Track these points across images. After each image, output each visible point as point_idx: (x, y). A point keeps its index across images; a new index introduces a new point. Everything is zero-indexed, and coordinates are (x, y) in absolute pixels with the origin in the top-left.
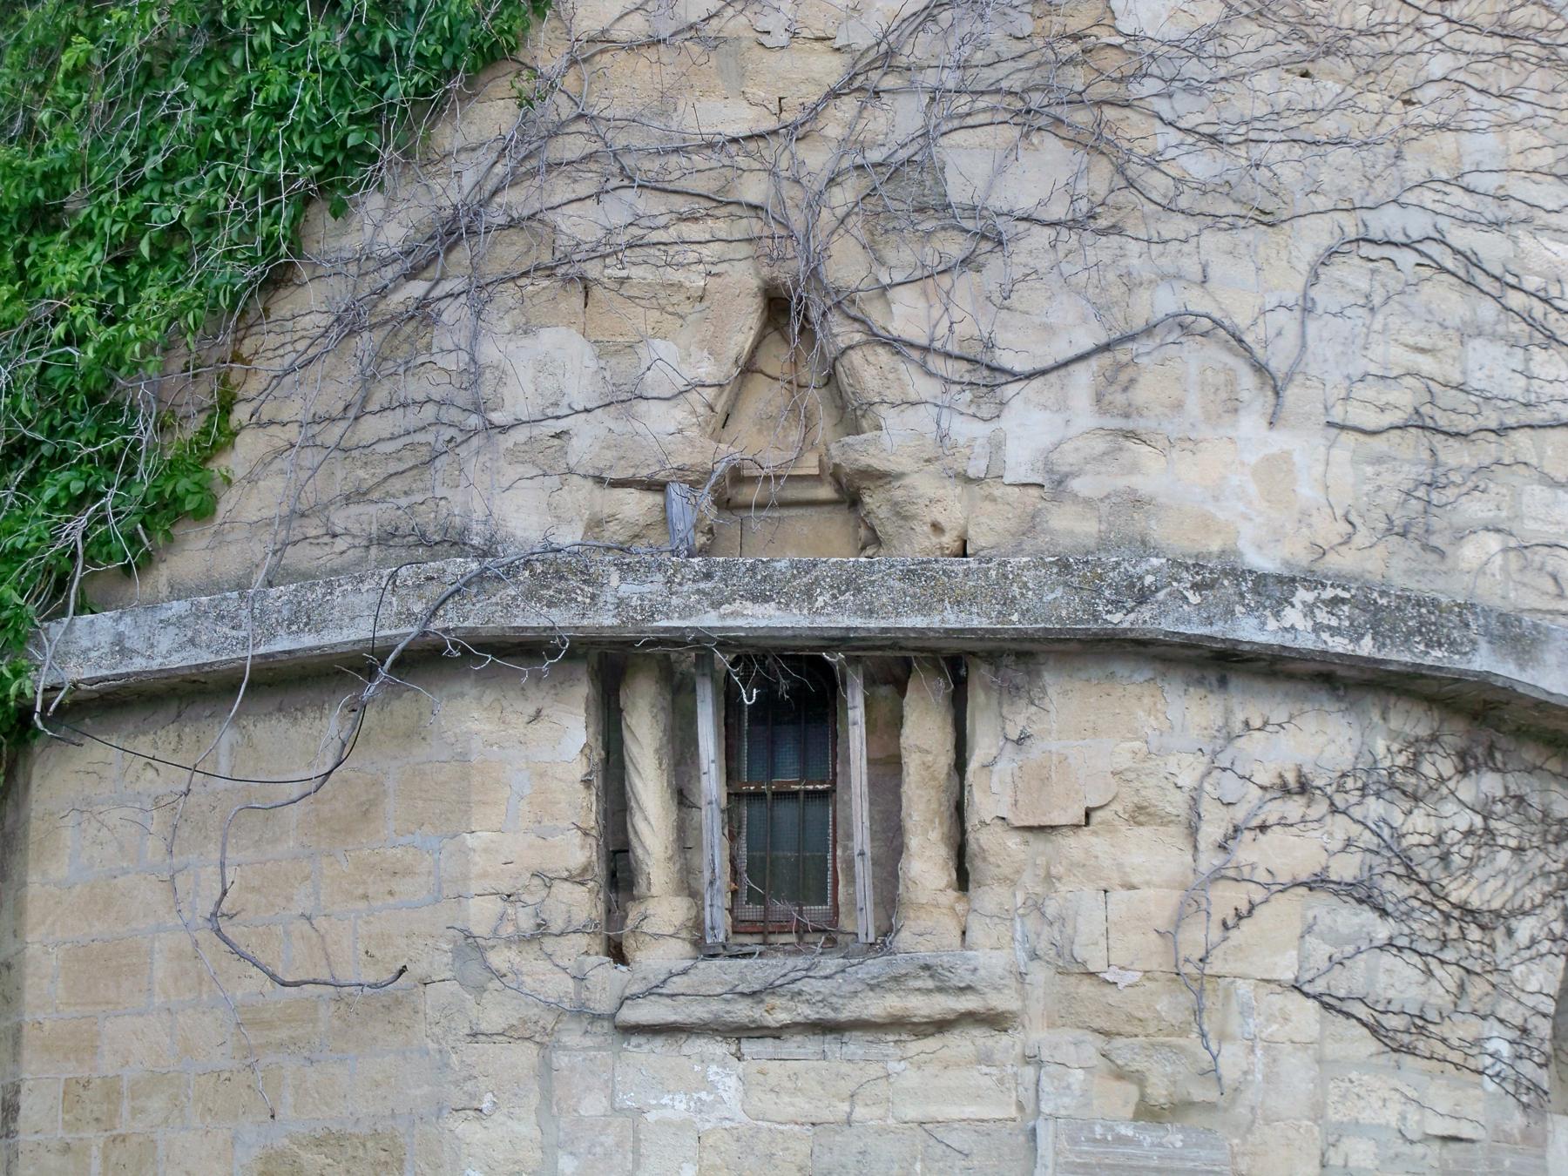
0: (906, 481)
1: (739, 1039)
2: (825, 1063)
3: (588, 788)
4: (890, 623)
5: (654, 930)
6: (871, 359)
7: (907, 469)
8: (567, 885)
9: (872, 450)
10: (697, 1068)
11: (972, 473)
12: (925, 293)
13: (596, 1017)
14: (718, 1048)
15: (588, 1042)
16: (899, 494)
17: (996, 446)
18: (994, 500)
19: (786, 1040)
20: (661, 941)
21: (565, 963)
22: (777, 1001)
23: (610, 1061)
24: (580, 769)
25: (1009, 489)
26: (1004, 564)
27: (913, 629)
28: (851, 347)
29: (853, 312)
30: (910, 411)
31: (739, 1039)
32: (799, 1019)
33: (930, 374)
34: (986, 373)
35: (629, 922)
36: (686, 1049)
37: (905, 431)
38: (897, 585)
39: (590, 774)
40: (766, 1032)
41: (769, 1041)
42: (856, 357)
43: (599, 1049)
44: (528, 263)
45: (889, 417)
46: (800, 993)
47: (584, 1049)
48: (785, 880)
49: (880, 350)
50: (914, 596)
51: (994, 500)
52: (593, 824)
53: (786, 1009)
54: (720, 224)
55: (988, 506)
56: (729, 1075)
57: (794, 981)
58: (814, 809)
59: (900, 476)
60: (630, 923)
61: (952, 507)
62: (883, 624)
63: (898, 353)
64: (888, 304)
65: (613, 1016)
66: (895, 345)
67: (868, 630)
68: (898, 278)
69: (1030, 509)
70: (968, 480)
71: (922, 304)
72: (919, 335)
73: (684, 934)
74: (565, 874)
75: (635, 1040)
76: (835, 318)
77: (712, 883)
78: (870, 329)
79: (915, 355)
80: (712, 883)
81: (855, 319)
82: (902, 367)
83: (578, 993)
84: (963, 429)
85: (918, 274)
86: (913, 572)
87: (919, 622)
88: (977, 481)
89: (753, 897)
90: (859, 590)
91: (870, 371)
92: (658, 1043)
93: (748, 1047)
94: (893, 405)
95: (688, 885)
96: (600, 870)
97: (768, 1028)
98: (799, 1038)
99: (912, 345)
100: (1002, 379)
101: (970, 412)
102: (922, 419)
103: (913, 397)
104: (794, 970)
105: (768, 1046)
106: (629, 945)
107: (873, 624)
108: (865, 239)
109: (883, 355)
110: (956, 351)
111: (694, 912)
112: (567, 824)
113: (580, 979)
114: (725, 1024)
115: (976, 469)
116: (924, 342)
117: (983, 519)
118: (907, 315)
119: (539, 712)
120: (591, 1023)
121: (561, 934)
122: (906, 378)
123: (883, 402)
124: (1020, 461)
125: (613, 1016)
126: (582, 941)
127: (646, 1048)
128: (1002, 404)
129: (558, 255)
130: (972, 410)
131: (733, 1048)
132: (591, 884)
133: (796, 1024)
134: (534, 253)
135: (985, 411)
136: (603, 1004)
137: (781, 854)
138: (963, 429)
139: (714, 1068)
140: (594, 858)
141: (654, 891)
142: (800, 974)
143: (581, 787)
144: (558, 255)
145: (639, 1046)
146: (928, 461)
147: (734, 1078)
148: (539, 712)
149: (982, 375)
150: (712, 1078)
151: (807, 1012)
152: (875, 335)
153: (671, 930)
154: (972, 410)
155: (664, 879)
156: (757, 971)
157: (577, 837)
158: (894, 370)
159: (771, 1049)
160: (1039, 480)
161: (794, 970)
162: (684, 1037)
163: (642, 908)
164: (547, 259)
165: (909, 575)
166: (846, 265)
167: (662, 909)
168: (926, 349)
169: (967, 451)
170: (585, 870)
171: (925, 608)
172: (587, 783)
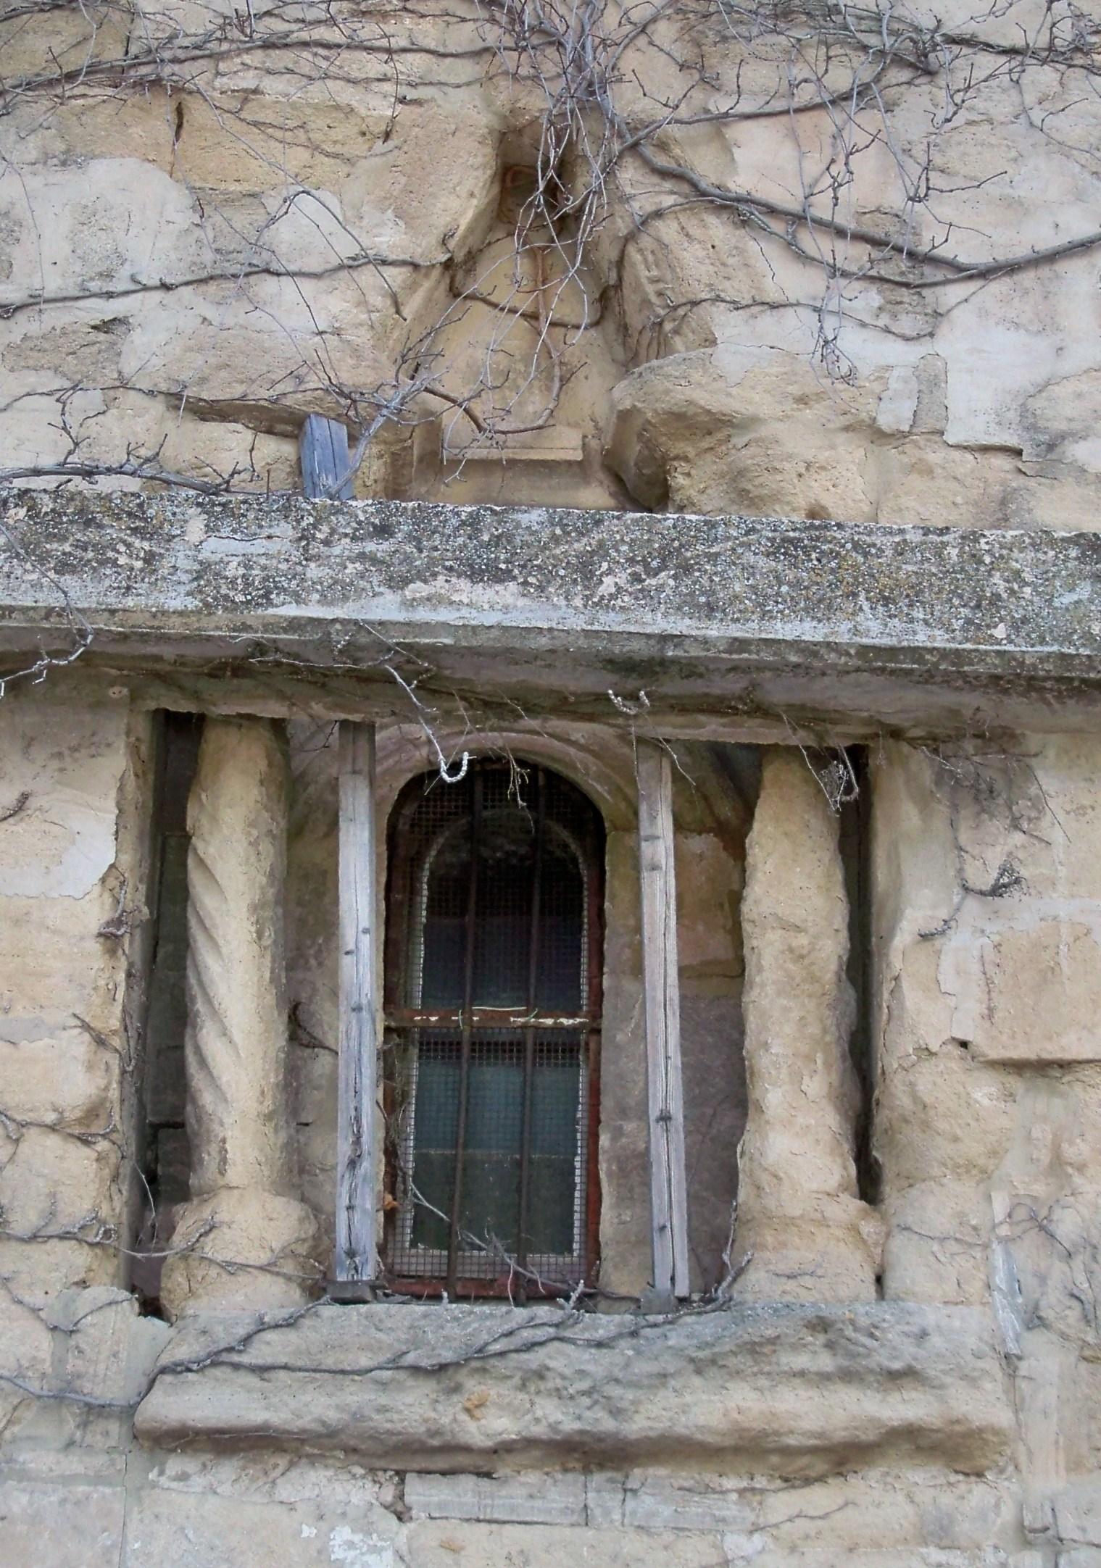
0: (763, 432)
1: (401, 1474)
2: (590, 1533)
3: (112, 952)
4: (750, 629)
5: (228, 1255)
6: (695, 232)
7: (764, 411)
8: (53, 1141)
9: (696, 376)
10: (308, 1532)
11: (885, 422)
12: (793, 135)
13: (94, 1411)
14: (358, 1492)
15: (74, 1464)
16: (746, 458)
17: (930, 383)
18: (928, 471)
19: (504, 1481)
20: (242, 1278)
21: (36, 1298)
22: (493, 1390)
23: (118, 1507)
24: (96, 913)
25: (957, 455)
26: (973, 537)
27: (796, 645)
28: (658, 214)
29: (661, 161)
30: (768, 320)
31: (401, 1474)
32: (539, 1431)
33: (804, 258)
34: (904, 263)
35: (176, 1238)
36: (285, 1490)
37: (759, 348)
38: (762, 562)
39: (118, 922)
40: (462, 1460)
41: (468, 1482)
42: (667, 230)
43: (98, 1480)
44: (80, 59)
45: (726, 324)
46: (540, 1374)
47: (68, 1480)
48: (493, 1195)
49: (712, 220)
50: (796, 584)
51: (928, 471)
52: (115, 1023)
53: (515, 1411)
54: (426, 24)
55: (916, 481)
56: (375, 1550)
57: (531, 1346)
58: (549, 1077)
59: (754, 421)
60: (178, 1241)
61: (844, 484)
62: (736, 631)
63: (744, 223)
64: (727, 148)
65: (131, 1409)
66: (739, 210)
67: (705, 642)
68: (746, 107)
69: (996, 490)
70: (878, 435)
71: (788, 151)
72: (785, 196)
73: (289, 1267)
74: (51, 1117)
75: (175, 1464)
76: (629, 174)
77: (353, 1164)
78: (694, 185)
79: (777, 226)
80: (353, 1164)
81: (664, 174)
82: (753, 247)
83: (59, 1361)
84: (863, 348)
85: (778, 105)
86: (795, 542)
87: (809, 631)
88: (896, 437)
89: (425, 1230)
90: (686, 569)
91: (696, 251)
92: (227, 1471)
93: (420, 1492)
94: (737, 306)
95: (298, 1175)
96: (121, 1121)
97: (467, 1449)
98: (532, 1477)
99: (772, 211)
100: (931, 273)
101: (881, 323)
102: (795, 330)
103: (773, 296)
104: (531, 1324)
105: (464, 1491)
106: (174, 1283)
107: (715, 630)
108: (683, 52)
109: (718, 228)
110: (851, 226)
111: (311, 1229)
112: (63, 1017)
113: (64, 1331)
114: (375, 1437)
115: (894, 415)
116: (794, 206)
117: (907, 502)
118: (761, 162)
119: (25, 797)
120: (84, 1425)
121: (34, 1238)
122: (761, 265)
123: (718, 299)
124: (974, 409)
125: (131, 1409)
126: (78, 1258)
127: (198, 1482)
128: (937, 314)
129: (134, 50)
130: (884, 320)
131: (388, 1494)
132: (103, 1145)
133: (529, 1443)
134: (91, 47)
135: (907, 324)
136: (111, 1386)
137: (479, 1154)
138: (863, 348)
139: (343, 1533)
140: (114, 1094)
141: (235, 1174)
142: (540, 1334)
143: (95, 947)
144: (134, 50)
145: (183, 1477)
146: (803, 400)
147: (388, 1556)
148: (25, 797)
149: (897, 268)
150: (338, 1554)
151: (554, 1416)
152: (704, 194)
153: (264, 1258)
154: (884, 320)
155: (253, 1154)
156: (451, 1325)
157: (80, 1045)
158: (740, 251)
159: (469, 1498)
160: (1012, 440)
161: (531, 1324)
162: (282, 1461)
163: (206, 1213)
164: (114, 53)
165: (785, 547)
166: (648, 84)
167: (244, 1216)
168: (798, 219)
169: (877, 387)
170: (93, 1112)
171: (820, 607)
172: (109, 939)
